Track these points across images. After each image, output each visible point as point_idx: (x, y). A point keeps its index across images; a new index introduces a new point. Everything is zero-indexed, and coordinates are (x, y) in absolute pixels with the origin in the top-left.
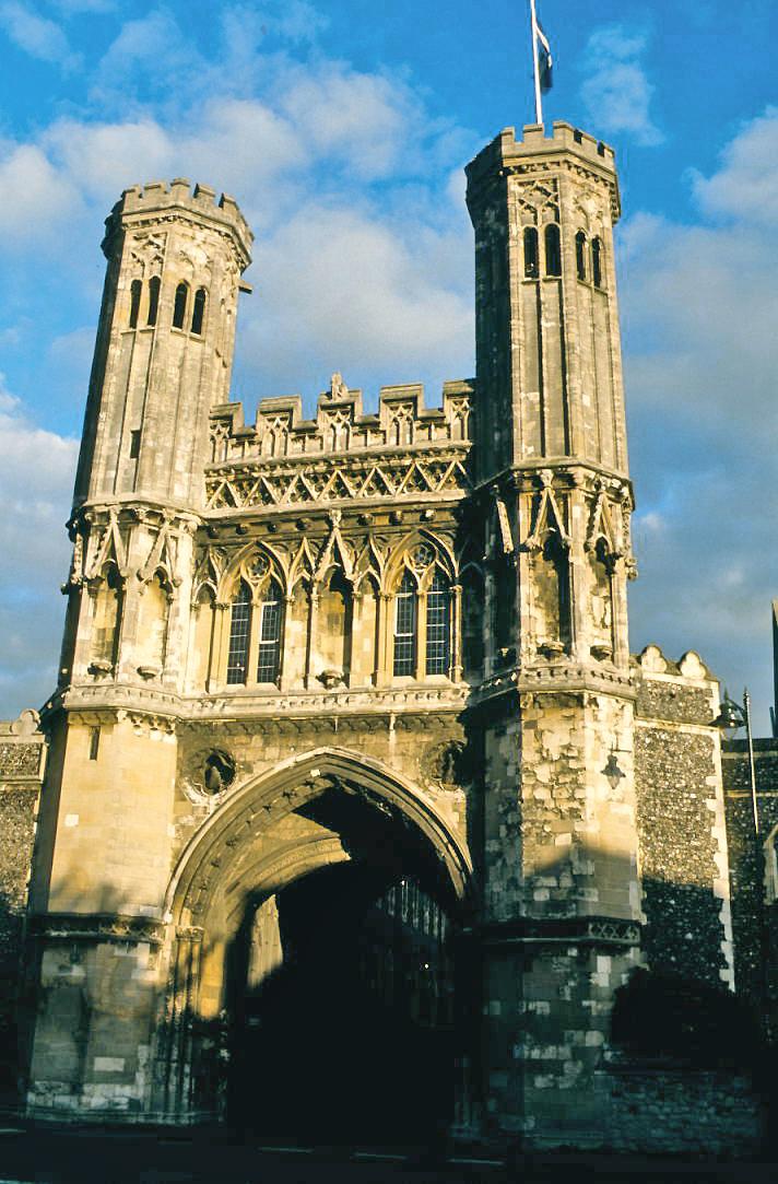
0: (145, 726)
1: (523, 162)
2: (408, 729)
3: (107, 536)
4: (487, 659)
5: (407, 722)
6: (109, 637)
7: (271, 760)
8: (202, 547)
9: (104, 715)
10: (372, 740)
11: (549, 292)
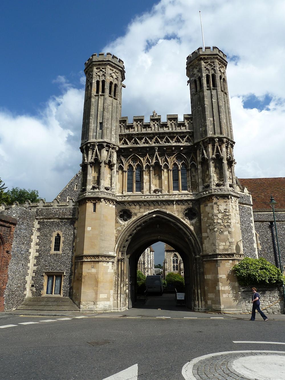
0: (108, 203)
1: (206, 57)
2: (179, 205)
3: (95, 151)
4: (200, 187)
5: (178, 202)
6: (96, 179)
7: (142, 212)
8: (118, 156)
9: (96, 200)
10: (169, 207)
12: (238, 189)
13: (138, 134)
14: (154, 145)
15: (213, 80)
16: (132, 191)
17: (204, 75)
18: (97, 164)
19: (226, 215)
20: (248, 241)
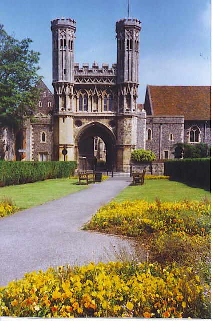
9: (64, 117)
11: (130, 53)
12: (139, 111)
13: (85, 76)
14: (94, 83)
15: (130, 42)
16: (82, 110)
17: (126, 39)
18: (64, 96)
19: (130, 127)
20: (140, 138)
